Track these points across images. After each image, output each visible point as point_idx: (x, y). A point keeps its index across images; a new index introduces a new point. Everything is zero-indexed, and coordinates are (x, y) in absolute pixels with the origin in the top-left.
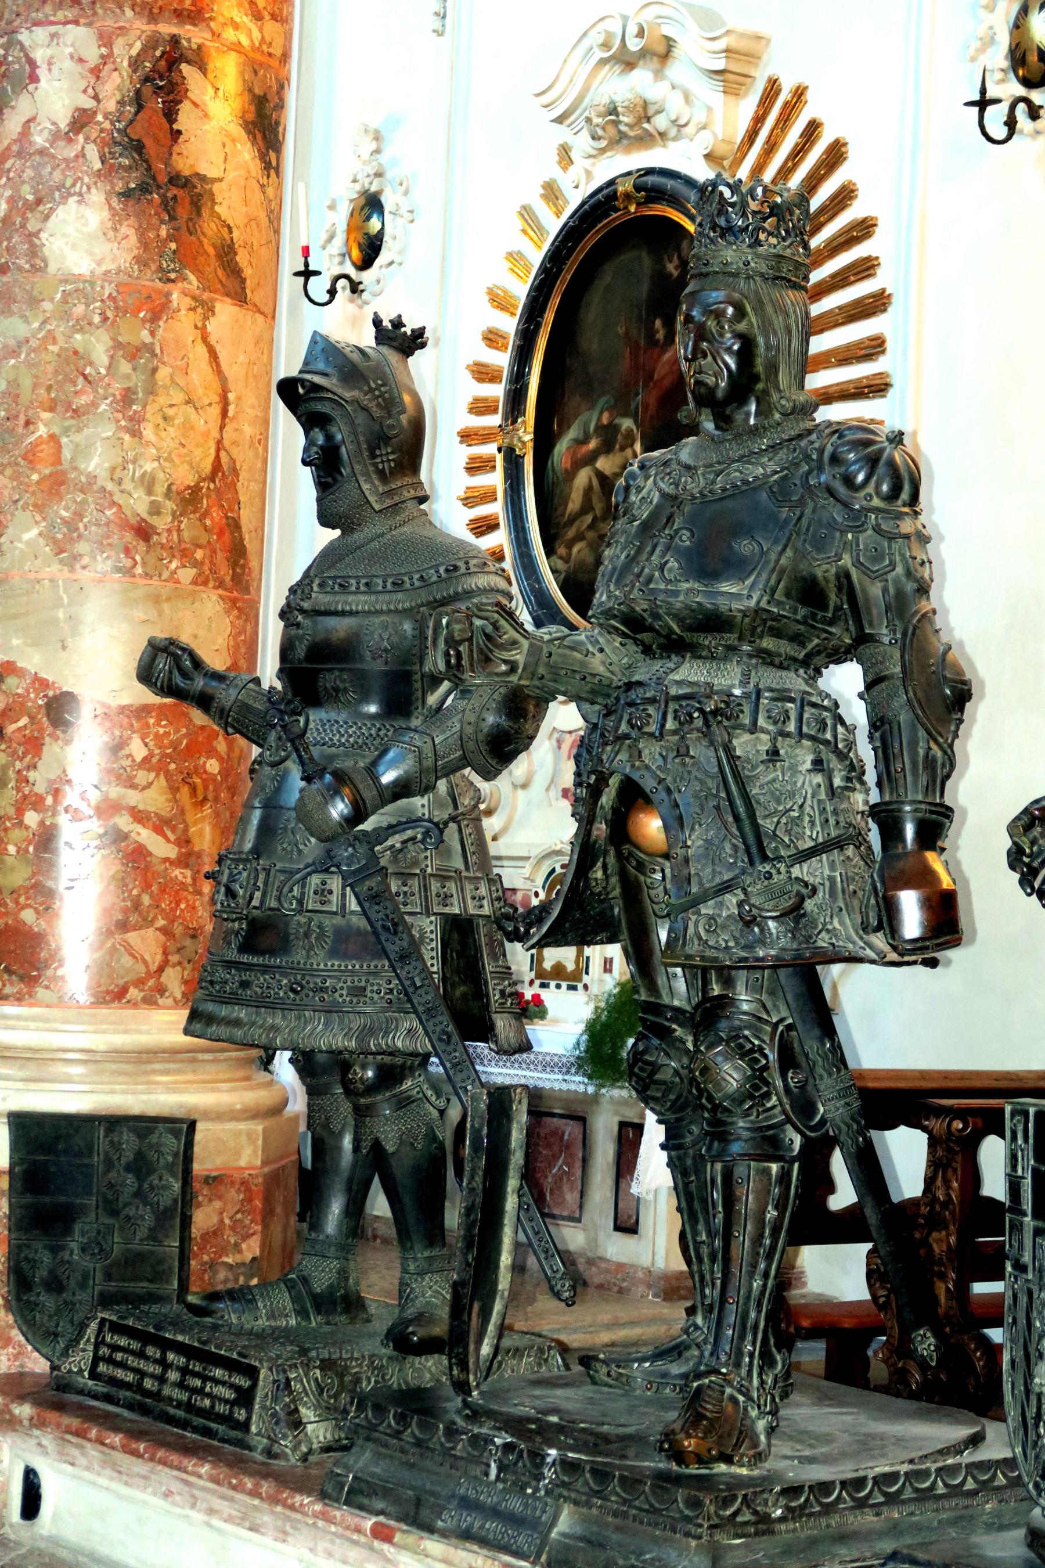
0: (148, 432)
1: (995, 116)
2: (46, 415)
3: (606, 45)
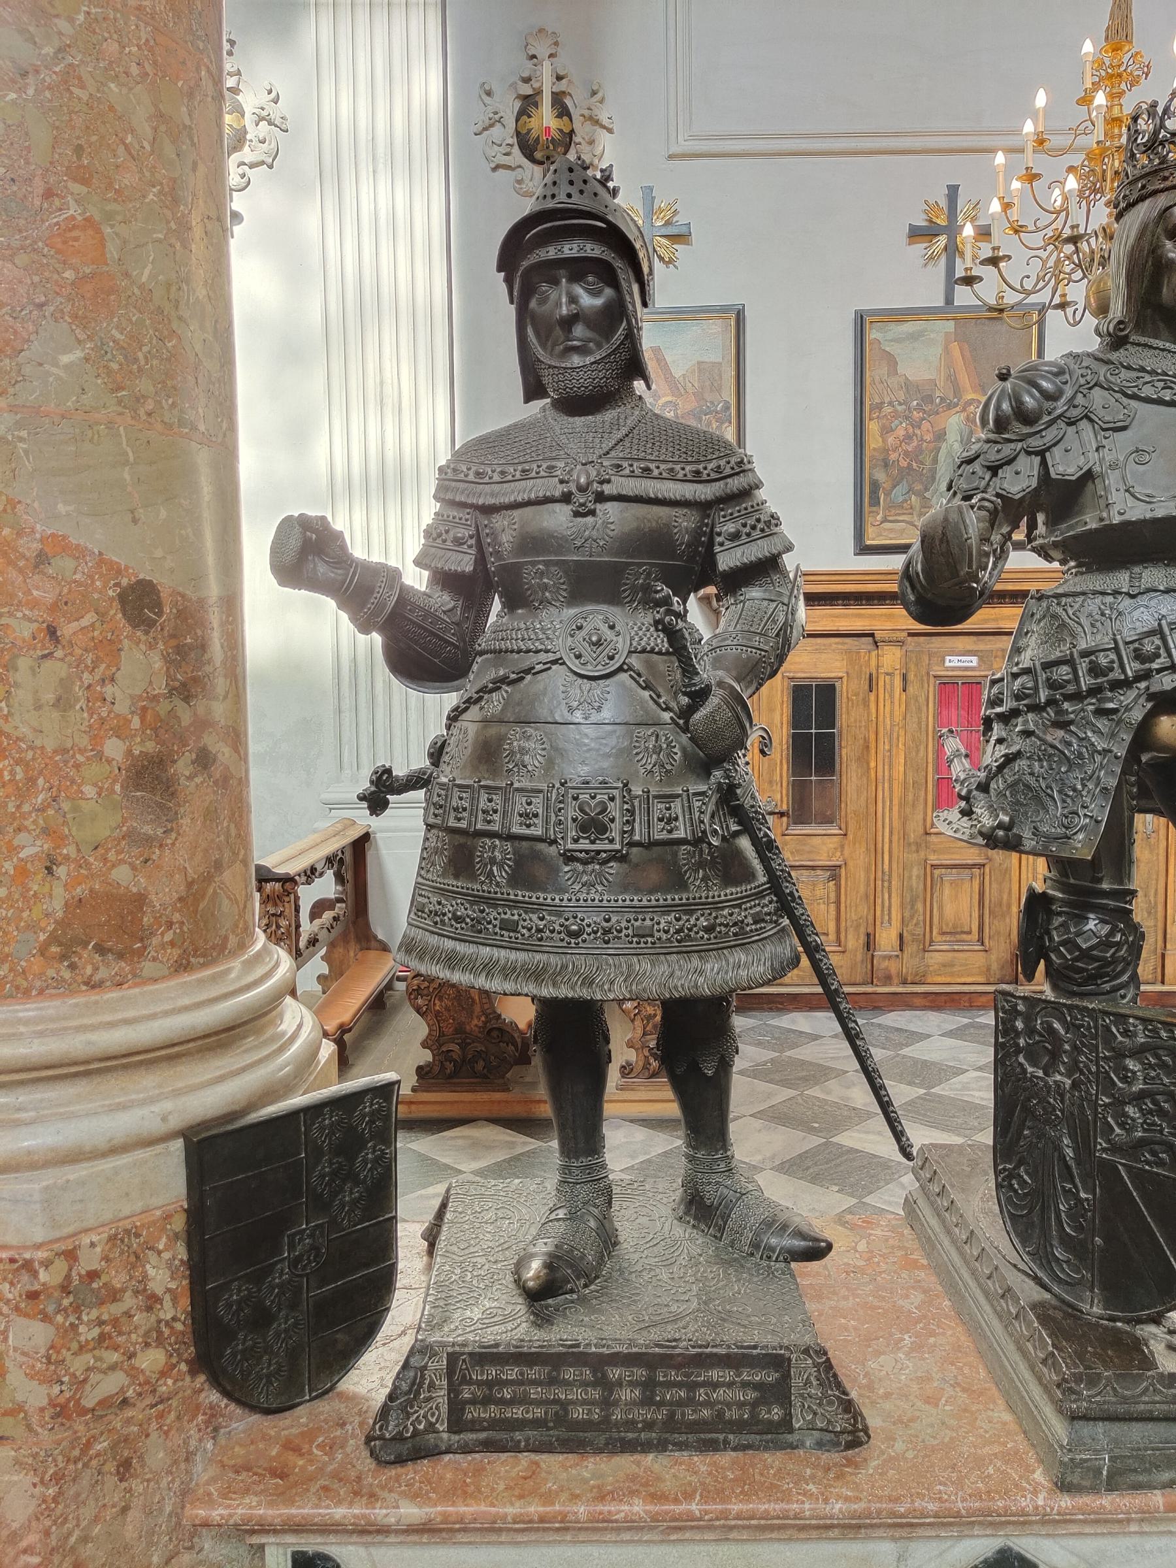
2: (77, 188)
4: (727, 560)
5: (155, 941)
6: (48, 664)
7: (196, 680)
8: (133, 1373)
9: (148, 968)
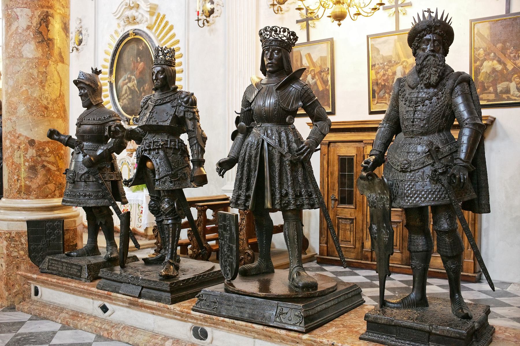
0: (46, 88)
1: (201, 23)
2: (25, 85)
3: (126, 5)
8: (19, 254)
9: (31, 197)
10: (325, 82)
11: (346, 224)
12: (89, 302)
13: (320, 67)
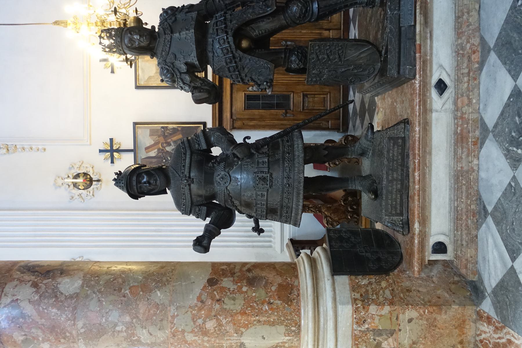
2: (123, 291)
4: (204, 146)
5: (290, 282)
6: (225, 302)
7: (230, 271)
8: (386, 288)
9: (296, 284)
10: (175, 130)
11: (309, 102)
12: (437, 120)
13: (159, 137)
